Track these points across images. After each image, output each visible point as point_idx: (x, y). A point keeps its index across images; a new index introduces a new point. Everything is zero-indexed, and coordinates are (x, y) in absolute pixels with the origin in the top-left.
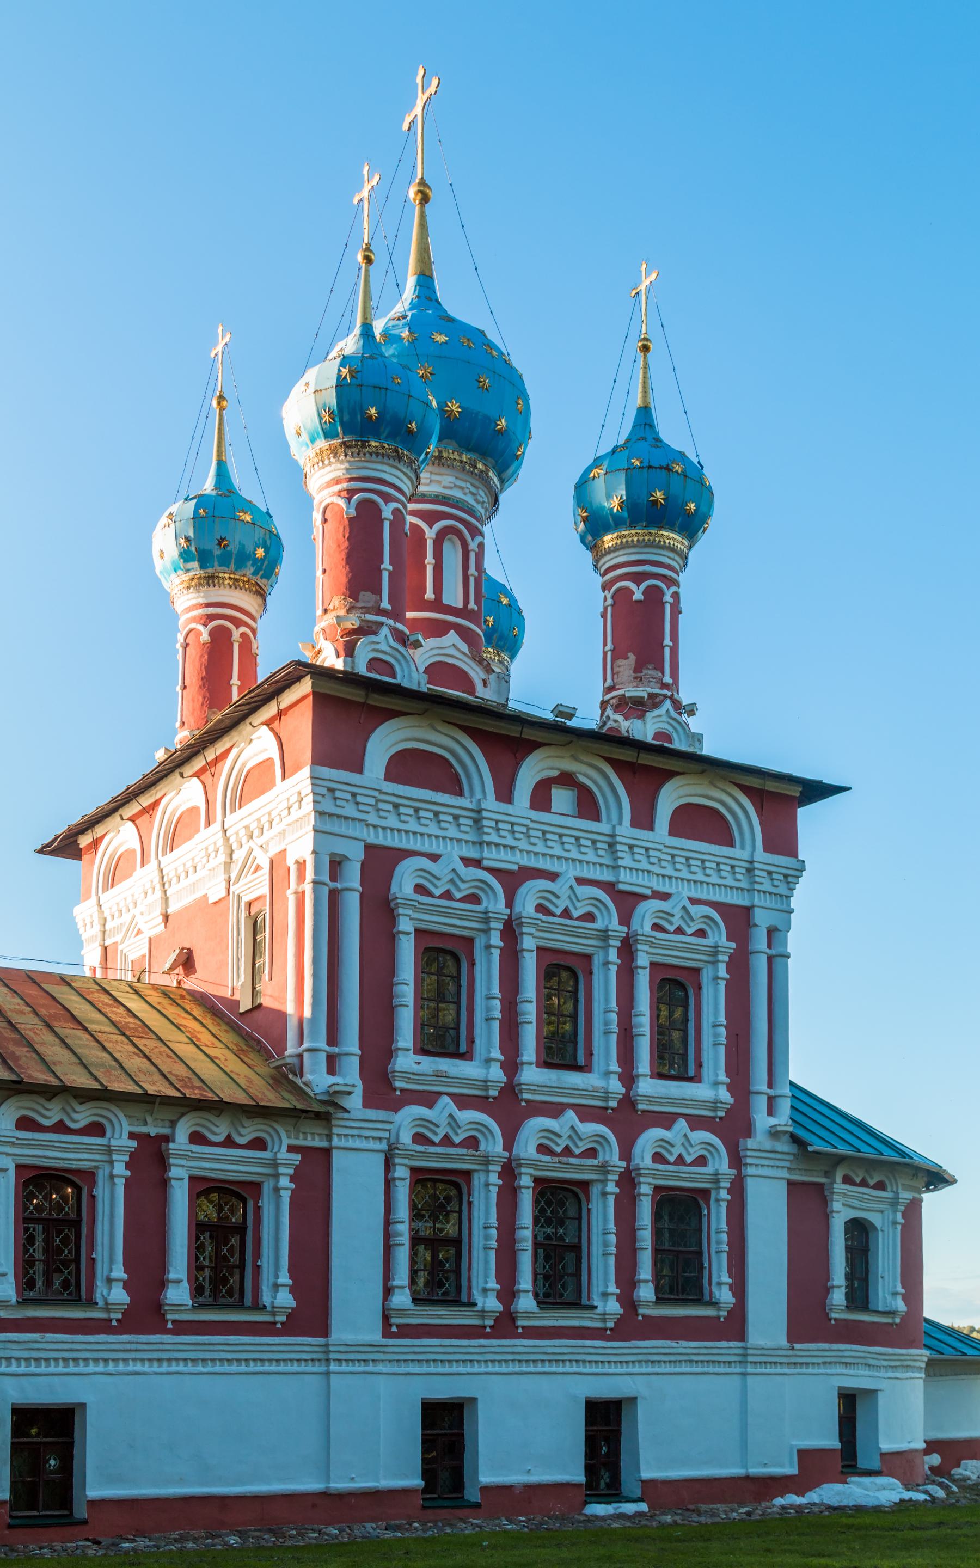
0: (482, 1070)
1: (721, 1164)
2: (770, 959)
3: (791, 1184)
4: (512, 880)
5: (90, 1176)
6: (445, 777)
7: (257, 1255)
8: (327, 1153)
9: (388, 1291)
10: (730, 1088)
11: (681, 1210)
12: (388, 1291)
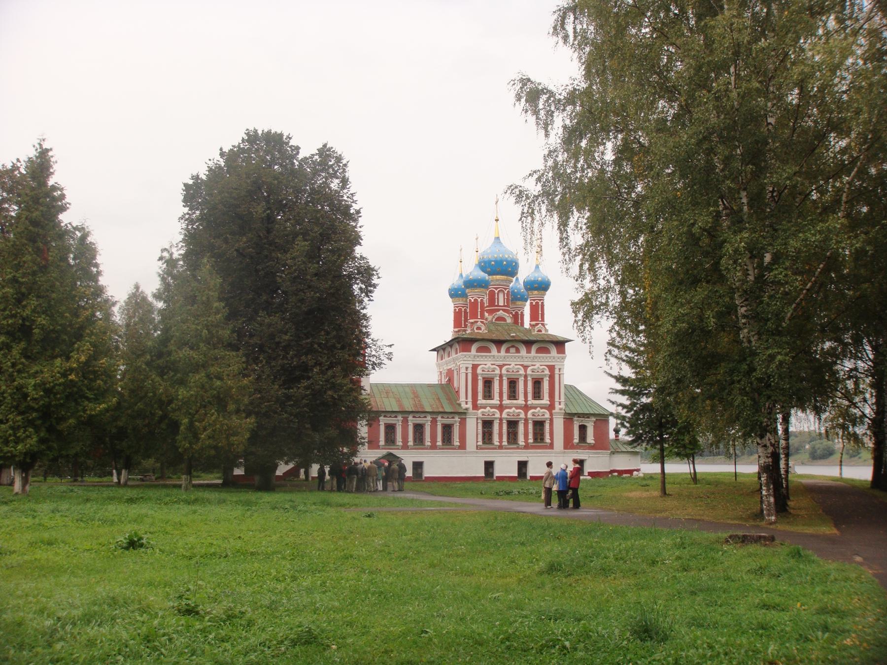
0: (496, 401)
1: (547, 415)
4: (501, 367)
6: (488, 350)
11: (539, 425)
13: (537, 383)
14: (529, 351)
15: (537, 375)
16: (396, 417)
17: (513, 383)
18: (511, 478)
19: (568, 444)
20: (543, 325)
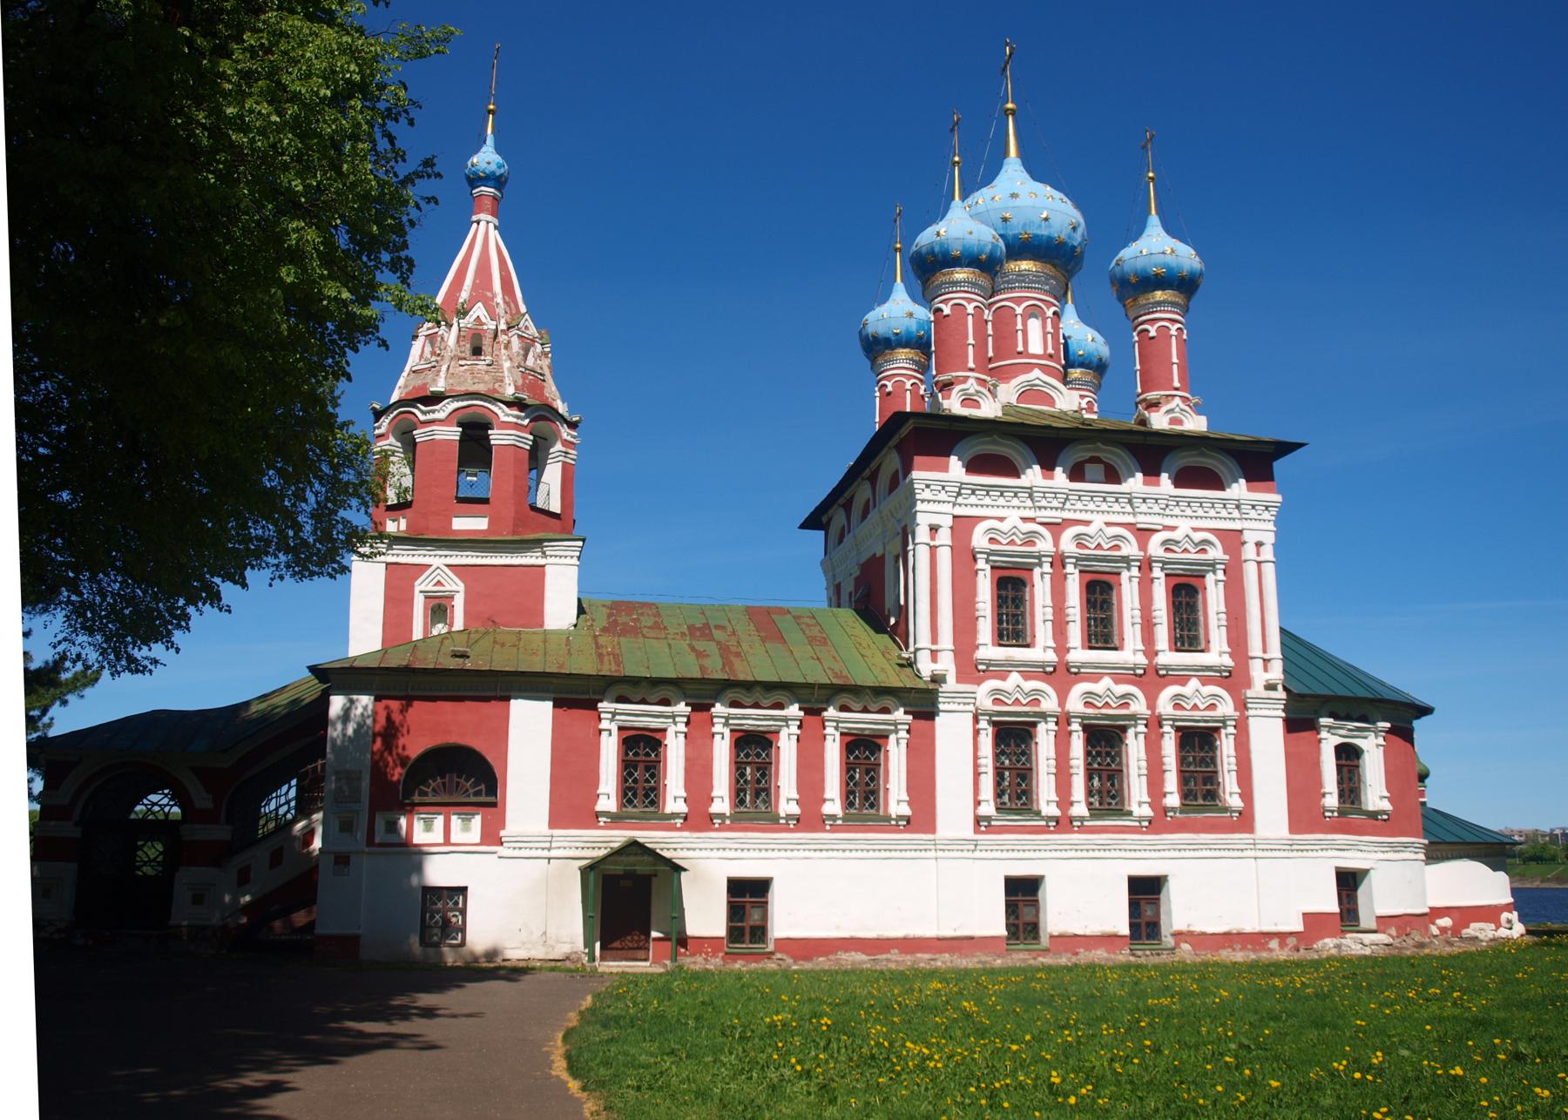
1: (1226, 708)
2: (1259, 563)
4: (1056, 528)
7: (886, 781)
9: (977, 803)
10: (1231, 655)
11: (1197, 741)
12: (977, 803)
13: (1185, 593)
16: (666, 702)
17: (1100, 592)
18: (1109, 939)
19: (1305, 815)
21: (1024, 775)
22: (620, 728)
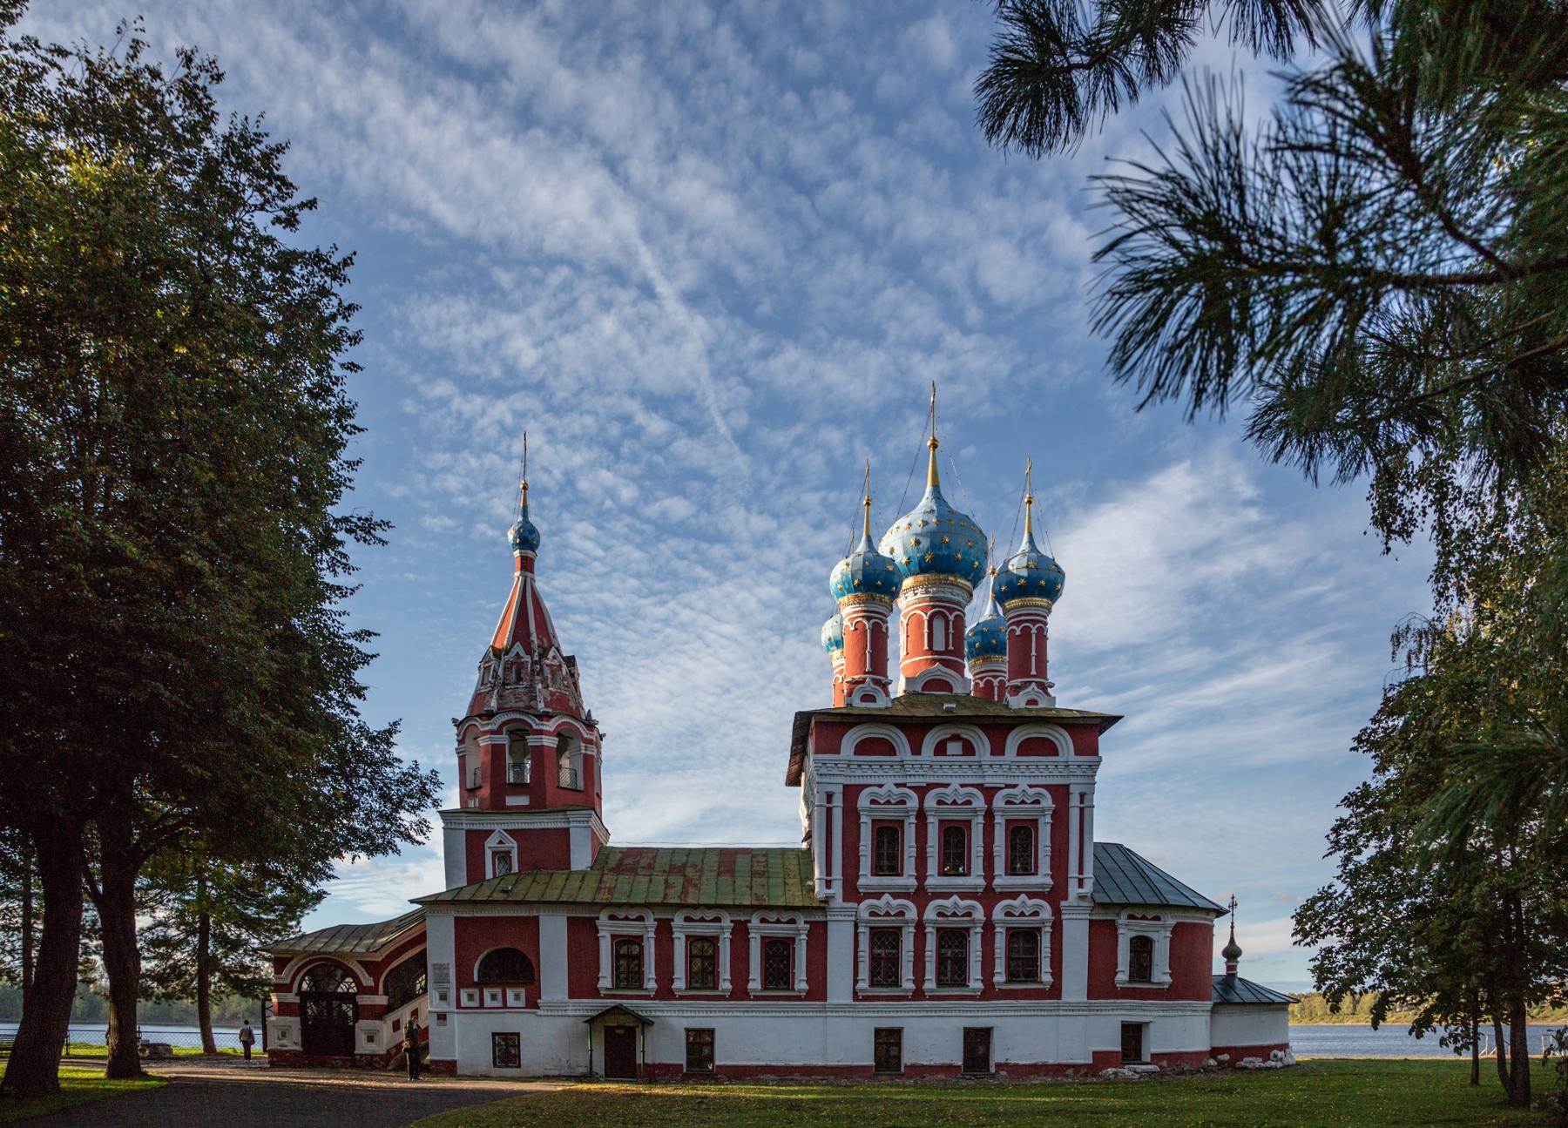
1: (1046, 913)
2: (1082, 810)
3: (1093, 924)
4: (922, 791)
5: (716, 938)
6: (887, 748)
8: (825, 923)
9: (856, 982)
12: (856, 982)
13: (1021, 833)
14: (998, 749)
15: (1021, 812)
16: (641, 919)
17: (955, 835)
18: (948, 1069)
19: (1101, 986)
20: (1044, 687)
21: (894, 962)
22: (613, 936)
